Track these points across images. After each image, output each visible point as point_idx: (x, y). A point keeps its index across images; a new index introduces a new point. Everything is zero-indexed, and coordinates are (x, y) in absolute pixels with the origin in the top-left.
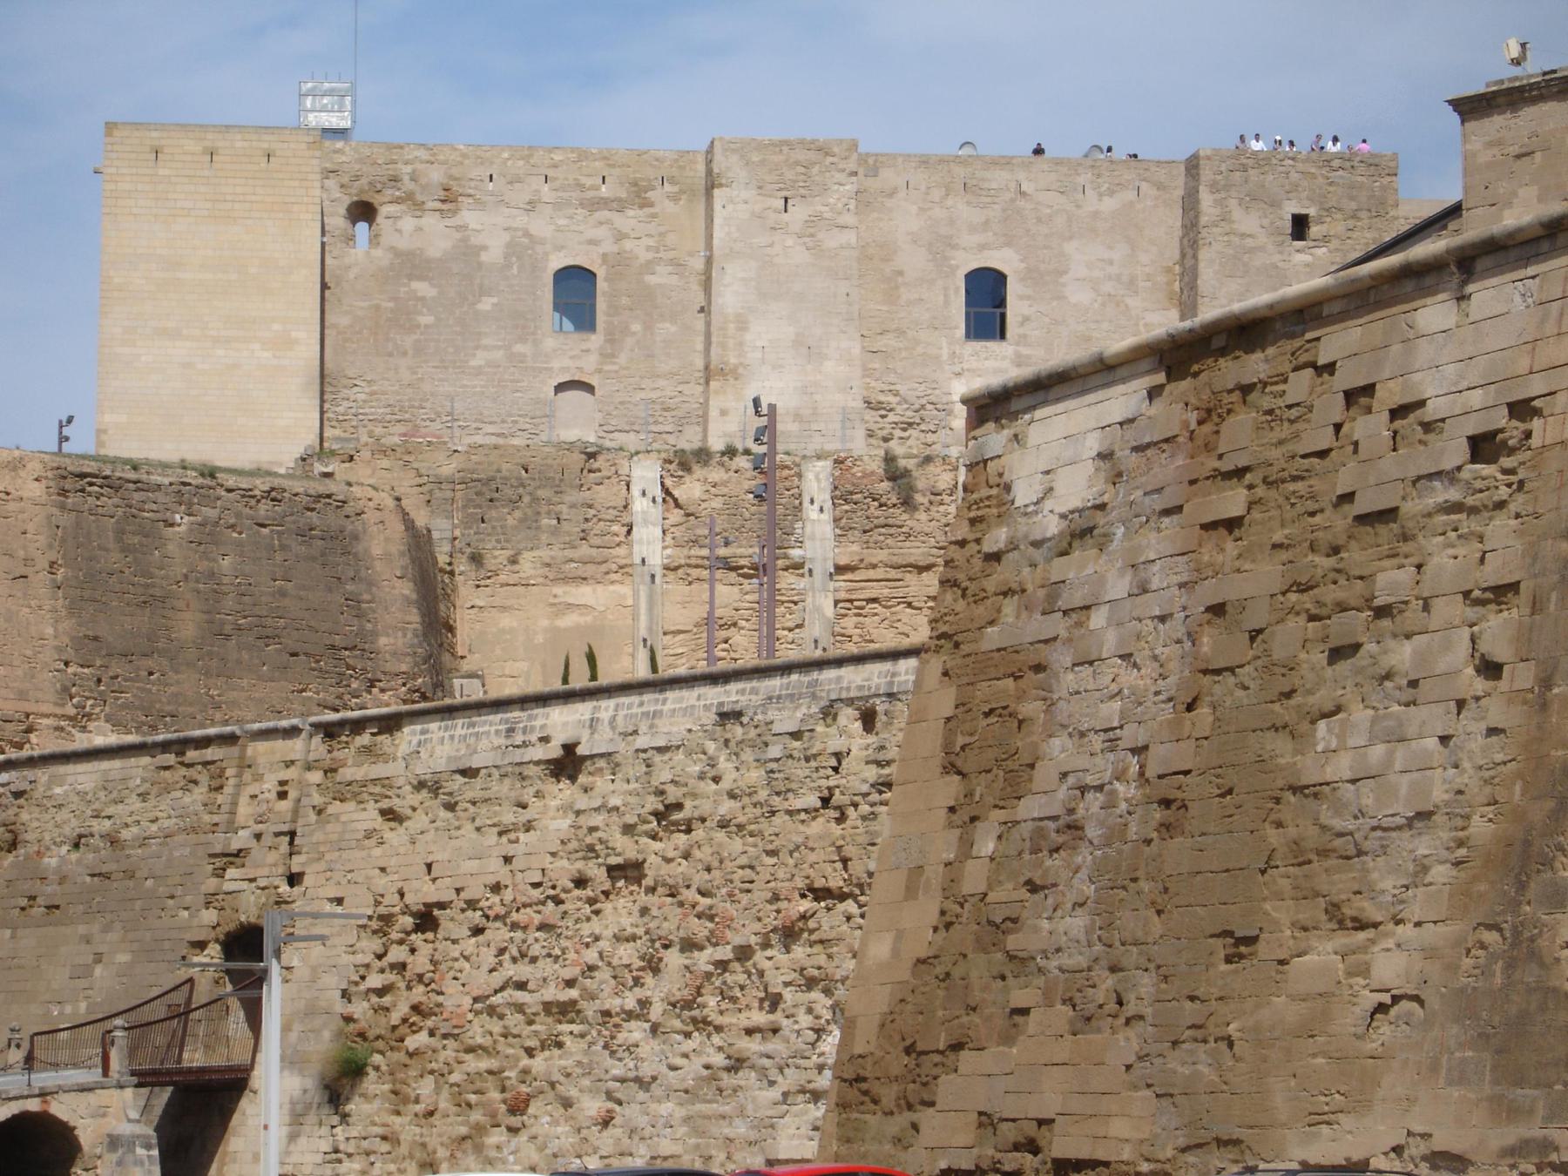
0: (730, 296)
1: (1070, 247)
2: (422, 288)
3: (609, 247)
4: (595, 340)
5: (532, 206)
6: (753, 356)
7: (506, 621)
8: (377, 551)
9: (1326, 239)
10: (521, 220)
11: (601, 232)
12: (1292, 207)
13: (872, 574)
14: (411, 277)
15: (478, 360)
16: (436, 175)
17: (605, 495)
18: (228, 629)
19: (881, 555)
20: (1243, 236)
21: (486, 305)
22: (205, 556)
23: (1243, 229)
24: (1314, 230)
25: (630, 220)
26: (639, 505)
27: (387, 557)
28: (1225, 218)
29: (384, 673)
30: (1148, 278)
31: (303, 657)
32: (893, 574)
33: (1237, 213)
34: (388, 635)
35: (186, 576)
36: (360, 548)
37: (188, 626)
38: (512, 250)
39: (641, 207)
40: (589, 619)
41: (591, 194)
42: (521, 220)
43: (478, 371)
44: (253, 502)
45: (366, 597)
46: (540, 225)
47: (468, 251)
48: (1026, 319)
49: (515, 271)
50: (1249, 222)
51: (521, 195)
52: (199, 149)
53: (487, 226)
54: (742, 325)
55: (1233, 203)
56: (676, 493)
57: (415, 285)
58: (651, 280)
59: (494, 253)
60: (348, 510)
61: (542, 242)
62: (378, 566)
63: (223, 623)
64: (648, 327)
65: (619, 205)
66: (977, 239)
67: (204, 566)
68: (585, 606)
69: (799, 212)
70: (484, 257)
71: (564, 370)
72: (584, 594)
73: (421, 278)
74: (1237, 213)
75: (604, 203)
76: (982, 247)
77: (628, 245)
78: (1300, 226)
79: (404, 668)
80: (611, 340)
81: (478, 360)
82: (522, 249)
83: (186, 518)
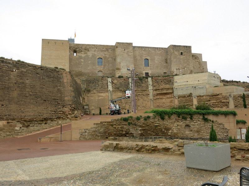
0: (118, 60)
1: (155, 57)
2: (82, 60)
3: (104, 56)
4: (103, 66)
5: (95, 51)
6: (121, 67)
7: (92, 98)
8: (65, 81)
9: (184, 55)
10: (93, 52)
11: (103, 54)
12: (181, 52)
13: (138, 91)
14: (80, 59)
15: (89, 68)
16: (84, 47)
17: (105, 82)
18: (27, 95)
19: (140, 89)
20: (176, 54)
21: (89, 62)
22: (21, 79)
23: (175, 53)
24: (183, 54)
25: (106, 53)
26: (109, 83)
27: (67, 82)
28: (174, 52)
29: (66, 104)
30: (164, 60)
31: (47, 101)
32: (141, 91)
33: (175, 52)
34: (67, 97)
35: (16, 83)
36: (62, 80)
37: (15, 94)
38: (92, 56)
39: (108, 51)
40: (103, 98)
41: (102, 50)
42: (93, 52)
43: (89, 70)
44: (36, 69)
45: (63, 90)
46: (96, 53)
47: (87, 56)
48: (151, 64)
49: (93, 58)
50: (176, 53)
51: (93, 50)
52: (54, 42)
53: (90, 54)
54: (120, 63)
55: (175, 51)
56: (113, 82)
57: (81, 60)
58: (109, 59)
59: (91, 56)
60: (59, 73)
61: (96, 55)
62: (65, 84)
63: (26, 94)
64: (109, 65)
65: (105, 51)
66: (145, 55)
67: (21, 81)
68: (102, 96)
69: (126, 51)
70: (89, 57)
71: (99, 70)
72: (102, 94)
73: (82, 59)
74: (175, 52)
75: (103, 51)
76: (146, 57)
77: (106, 55)
78: (182, 53)
79: (70, 103)
80: (104, 66)
81: (89, 68)
82: (94, 56)
83: (17, 71)
